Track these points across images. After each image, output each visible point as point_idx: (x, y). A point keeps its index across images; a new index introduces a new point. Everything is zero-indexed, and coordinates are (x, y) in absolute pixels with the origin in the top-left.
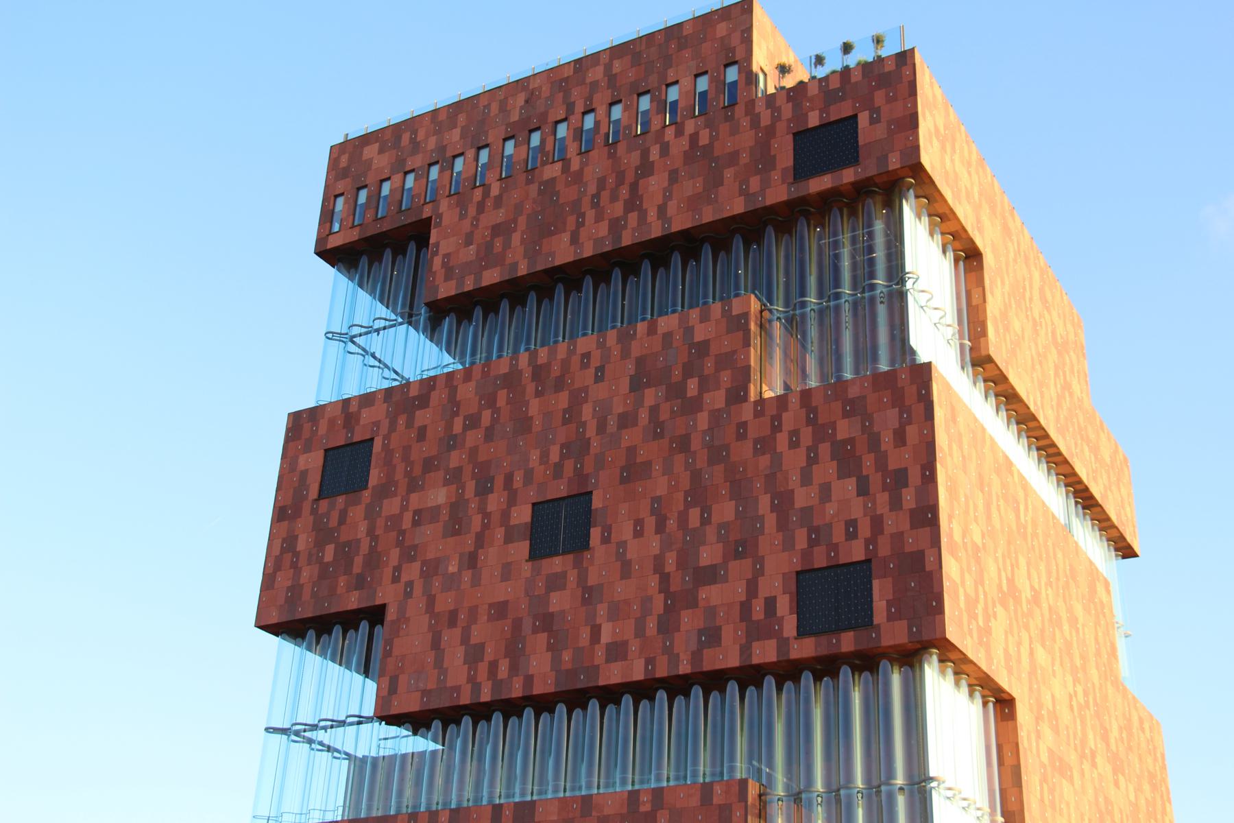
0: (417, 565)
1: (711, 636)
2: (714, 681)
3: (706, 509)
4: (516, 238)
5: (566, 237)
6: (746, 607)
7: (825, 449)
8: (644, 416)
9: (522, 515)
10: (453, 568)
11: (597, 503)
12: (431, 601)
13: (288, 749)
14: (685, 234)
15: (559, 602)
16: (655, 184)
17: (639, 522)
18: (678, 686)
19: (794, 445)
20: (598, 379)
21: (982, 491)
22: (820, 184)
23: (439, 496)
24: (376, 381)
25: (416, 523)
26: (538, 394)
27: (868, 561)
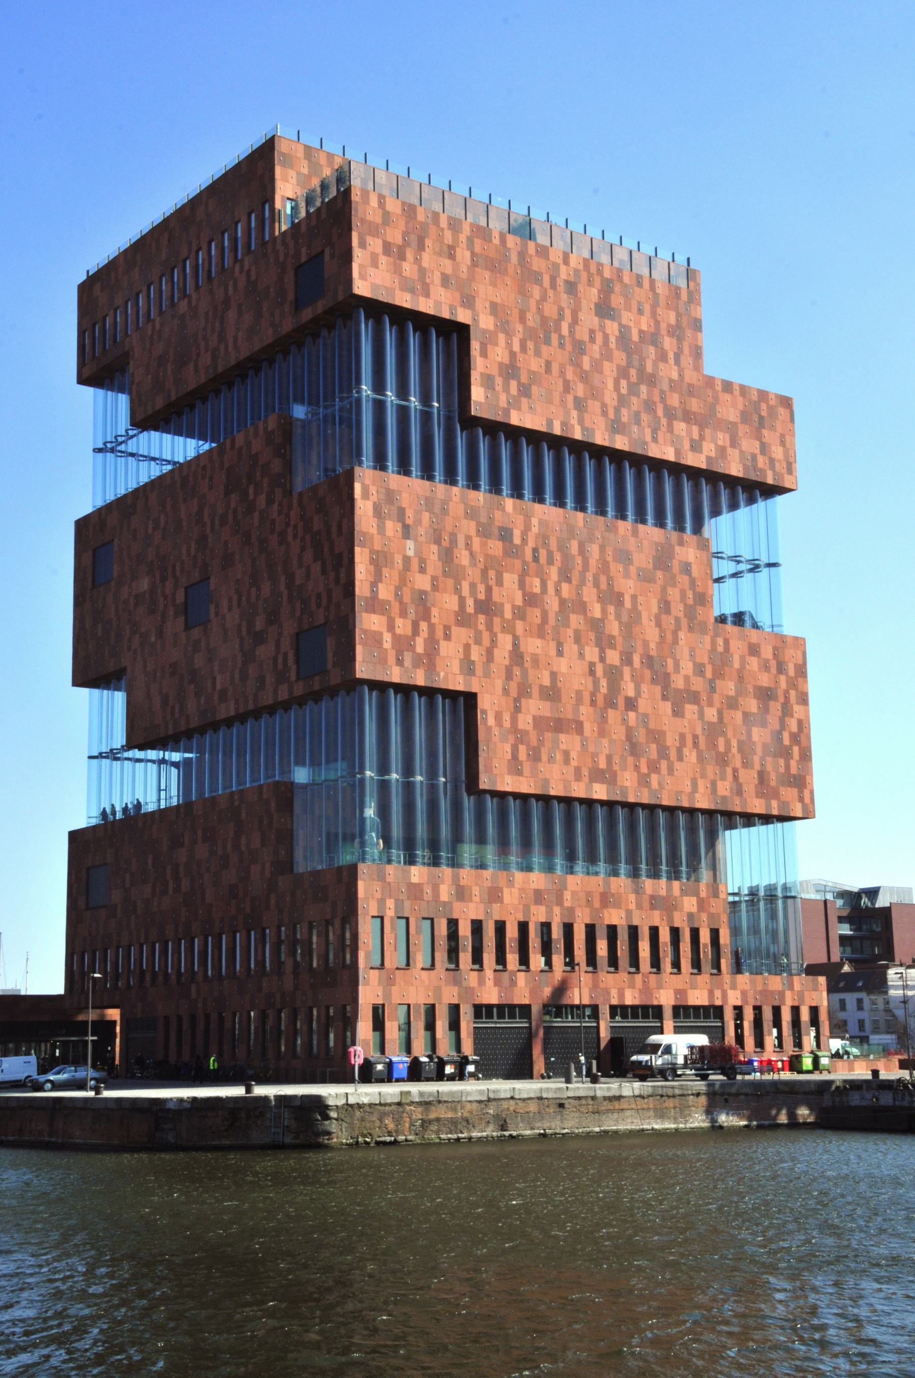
0: (137, 636)
1: (262, 680)
2: (271, 710)
3: (259, 589)
4: (169, 365)
5: (191, 366)
6: (275, 659)
7: (308, 537)
8: (230, 517)
9: (180, 597)
10: (153, 639)
11: (212, 587)
12: (145, 666)
13: (111, 766)
14: (249, 359)
15: (199, 661)
16: (232, 315)
17: (230, 600)
18: (256, 714)
19: (295, 536)
20: (211, 488)
21: (438, 541)
22: (307, 314)
23: (144, 584)
24: (147, 473)
25: (136, 605)
26: (185, 501)
27: (326, 623)
